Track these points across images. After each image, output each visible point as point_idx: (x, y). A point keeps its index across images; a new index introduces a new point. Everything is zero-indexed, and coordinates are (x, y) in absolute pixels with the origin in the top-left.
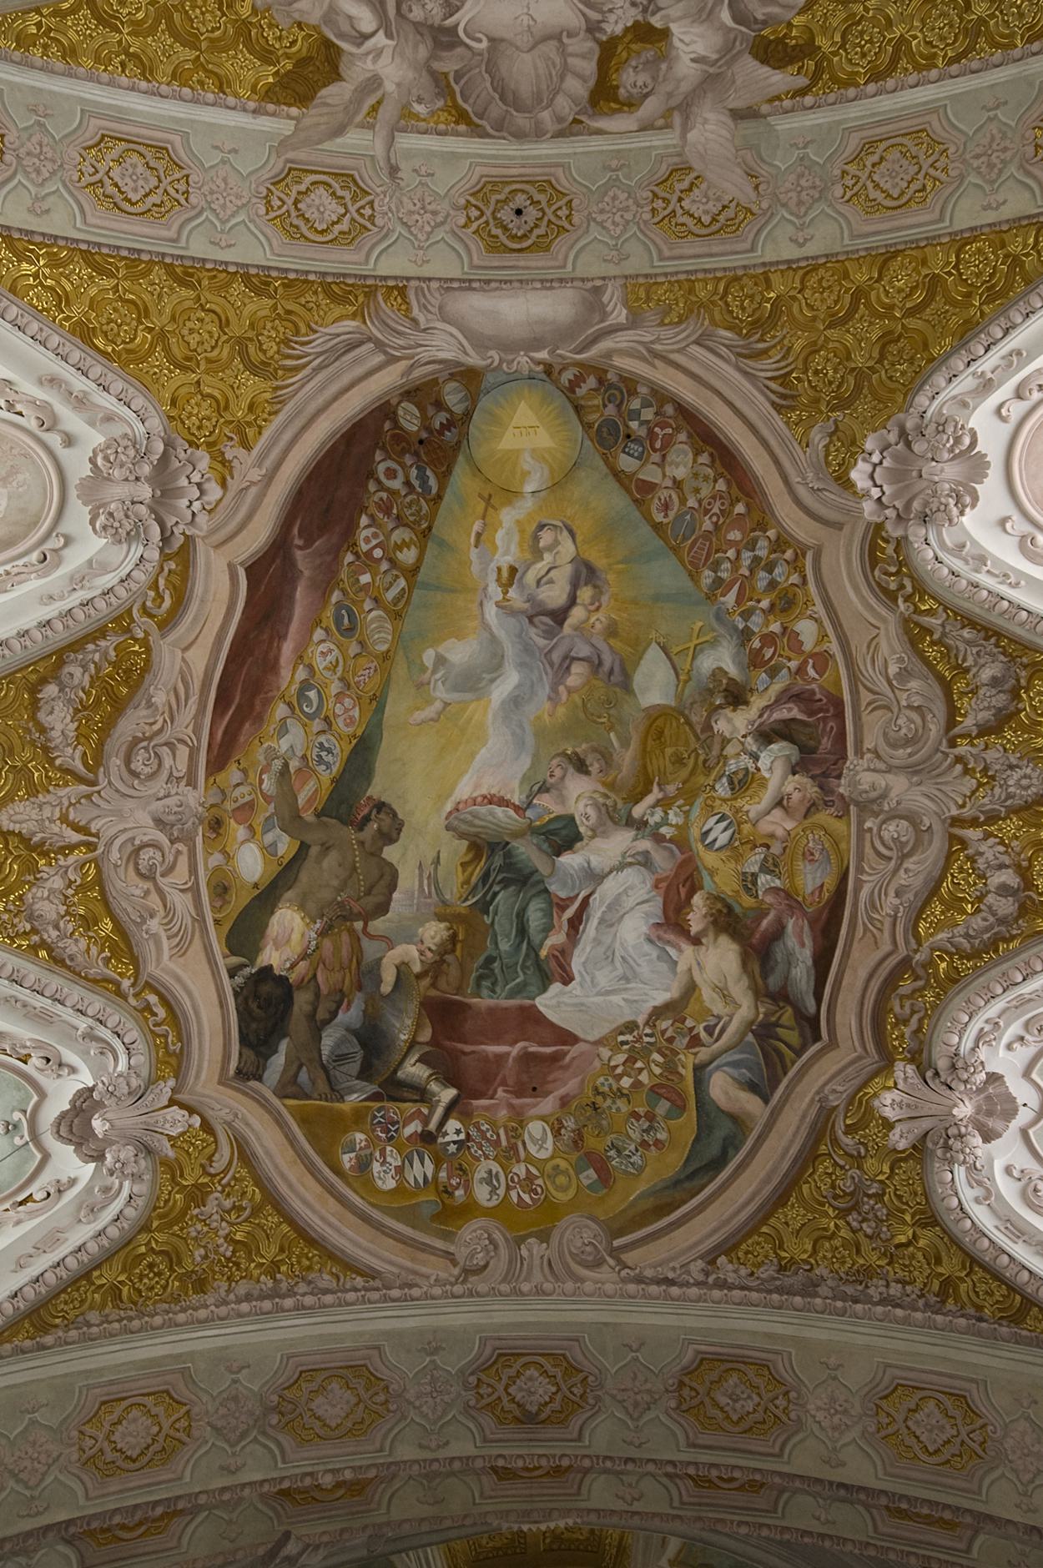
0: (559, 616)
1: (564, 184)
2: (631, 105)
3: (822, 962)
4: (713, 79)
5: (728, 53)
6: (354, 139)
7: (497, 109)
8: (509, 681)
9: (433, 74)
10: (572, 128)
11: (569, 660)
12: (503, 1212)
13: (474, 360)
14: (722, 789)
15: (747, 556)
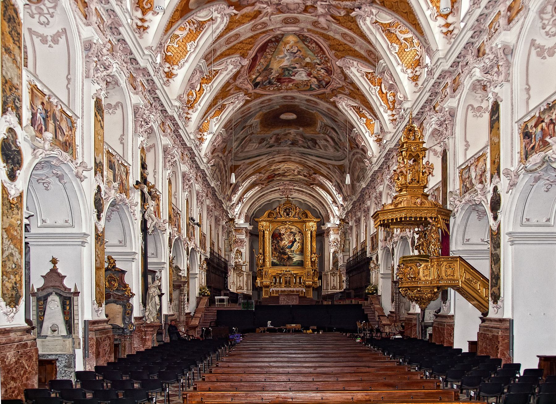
0: (295, 53)
1: (298, 18)
2: (310, 13)
3: (326, 85)
4: (323, 15)
5: (326, 13)
6: (264, 19)
7: (287, 10)
8: (288, 57)
9: (277, 9)
10: (300, 13)
11: (296, 57)
12: (286, 89)
13: (283, 33)
14: (316, 70)
15: (322, 56)
